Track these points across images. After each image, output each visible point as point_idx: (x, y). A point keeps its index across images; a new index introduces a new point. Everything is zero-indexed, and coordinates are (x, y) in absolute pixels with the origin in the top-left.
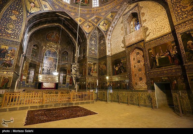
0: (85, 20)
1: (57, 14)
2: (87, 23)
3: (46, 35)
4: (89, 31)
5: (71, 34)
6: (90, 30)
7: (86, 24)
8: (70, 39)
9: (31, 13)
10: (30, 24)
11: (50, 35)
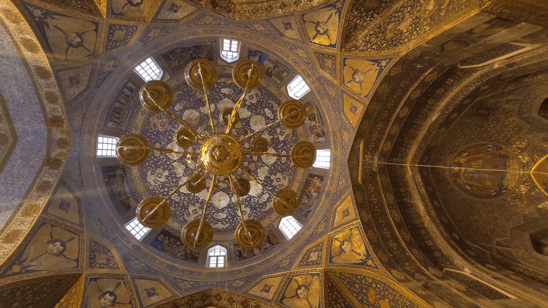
0: (345, 96)
1: (363, 180)
2: (349, 85)
3: (474, 199)
4: (371, 67)
5: (426, 117)
6: (364, 65)
7: (354, 87)
8: (452, 113)
9: (366, 254)
10: (409, 259)
11: (471, 186)
